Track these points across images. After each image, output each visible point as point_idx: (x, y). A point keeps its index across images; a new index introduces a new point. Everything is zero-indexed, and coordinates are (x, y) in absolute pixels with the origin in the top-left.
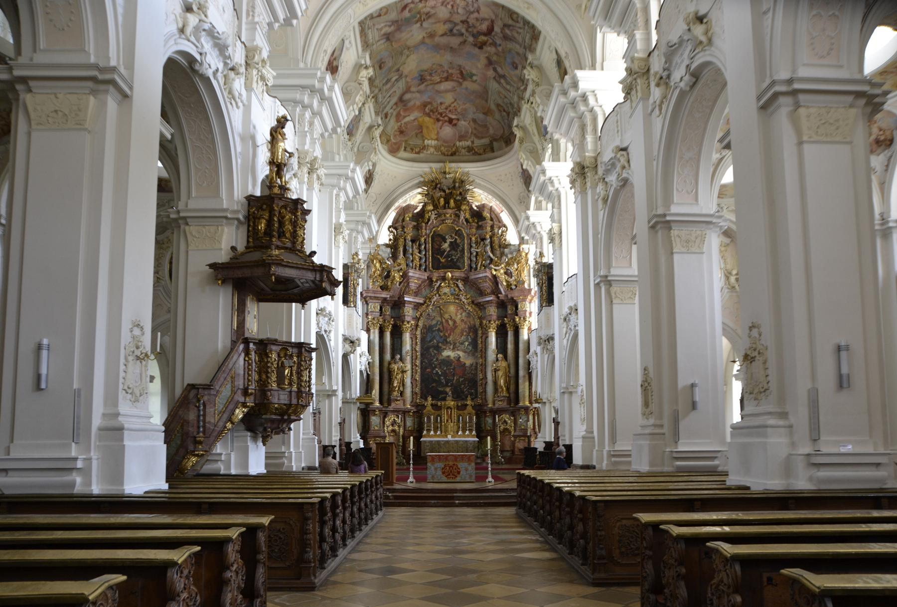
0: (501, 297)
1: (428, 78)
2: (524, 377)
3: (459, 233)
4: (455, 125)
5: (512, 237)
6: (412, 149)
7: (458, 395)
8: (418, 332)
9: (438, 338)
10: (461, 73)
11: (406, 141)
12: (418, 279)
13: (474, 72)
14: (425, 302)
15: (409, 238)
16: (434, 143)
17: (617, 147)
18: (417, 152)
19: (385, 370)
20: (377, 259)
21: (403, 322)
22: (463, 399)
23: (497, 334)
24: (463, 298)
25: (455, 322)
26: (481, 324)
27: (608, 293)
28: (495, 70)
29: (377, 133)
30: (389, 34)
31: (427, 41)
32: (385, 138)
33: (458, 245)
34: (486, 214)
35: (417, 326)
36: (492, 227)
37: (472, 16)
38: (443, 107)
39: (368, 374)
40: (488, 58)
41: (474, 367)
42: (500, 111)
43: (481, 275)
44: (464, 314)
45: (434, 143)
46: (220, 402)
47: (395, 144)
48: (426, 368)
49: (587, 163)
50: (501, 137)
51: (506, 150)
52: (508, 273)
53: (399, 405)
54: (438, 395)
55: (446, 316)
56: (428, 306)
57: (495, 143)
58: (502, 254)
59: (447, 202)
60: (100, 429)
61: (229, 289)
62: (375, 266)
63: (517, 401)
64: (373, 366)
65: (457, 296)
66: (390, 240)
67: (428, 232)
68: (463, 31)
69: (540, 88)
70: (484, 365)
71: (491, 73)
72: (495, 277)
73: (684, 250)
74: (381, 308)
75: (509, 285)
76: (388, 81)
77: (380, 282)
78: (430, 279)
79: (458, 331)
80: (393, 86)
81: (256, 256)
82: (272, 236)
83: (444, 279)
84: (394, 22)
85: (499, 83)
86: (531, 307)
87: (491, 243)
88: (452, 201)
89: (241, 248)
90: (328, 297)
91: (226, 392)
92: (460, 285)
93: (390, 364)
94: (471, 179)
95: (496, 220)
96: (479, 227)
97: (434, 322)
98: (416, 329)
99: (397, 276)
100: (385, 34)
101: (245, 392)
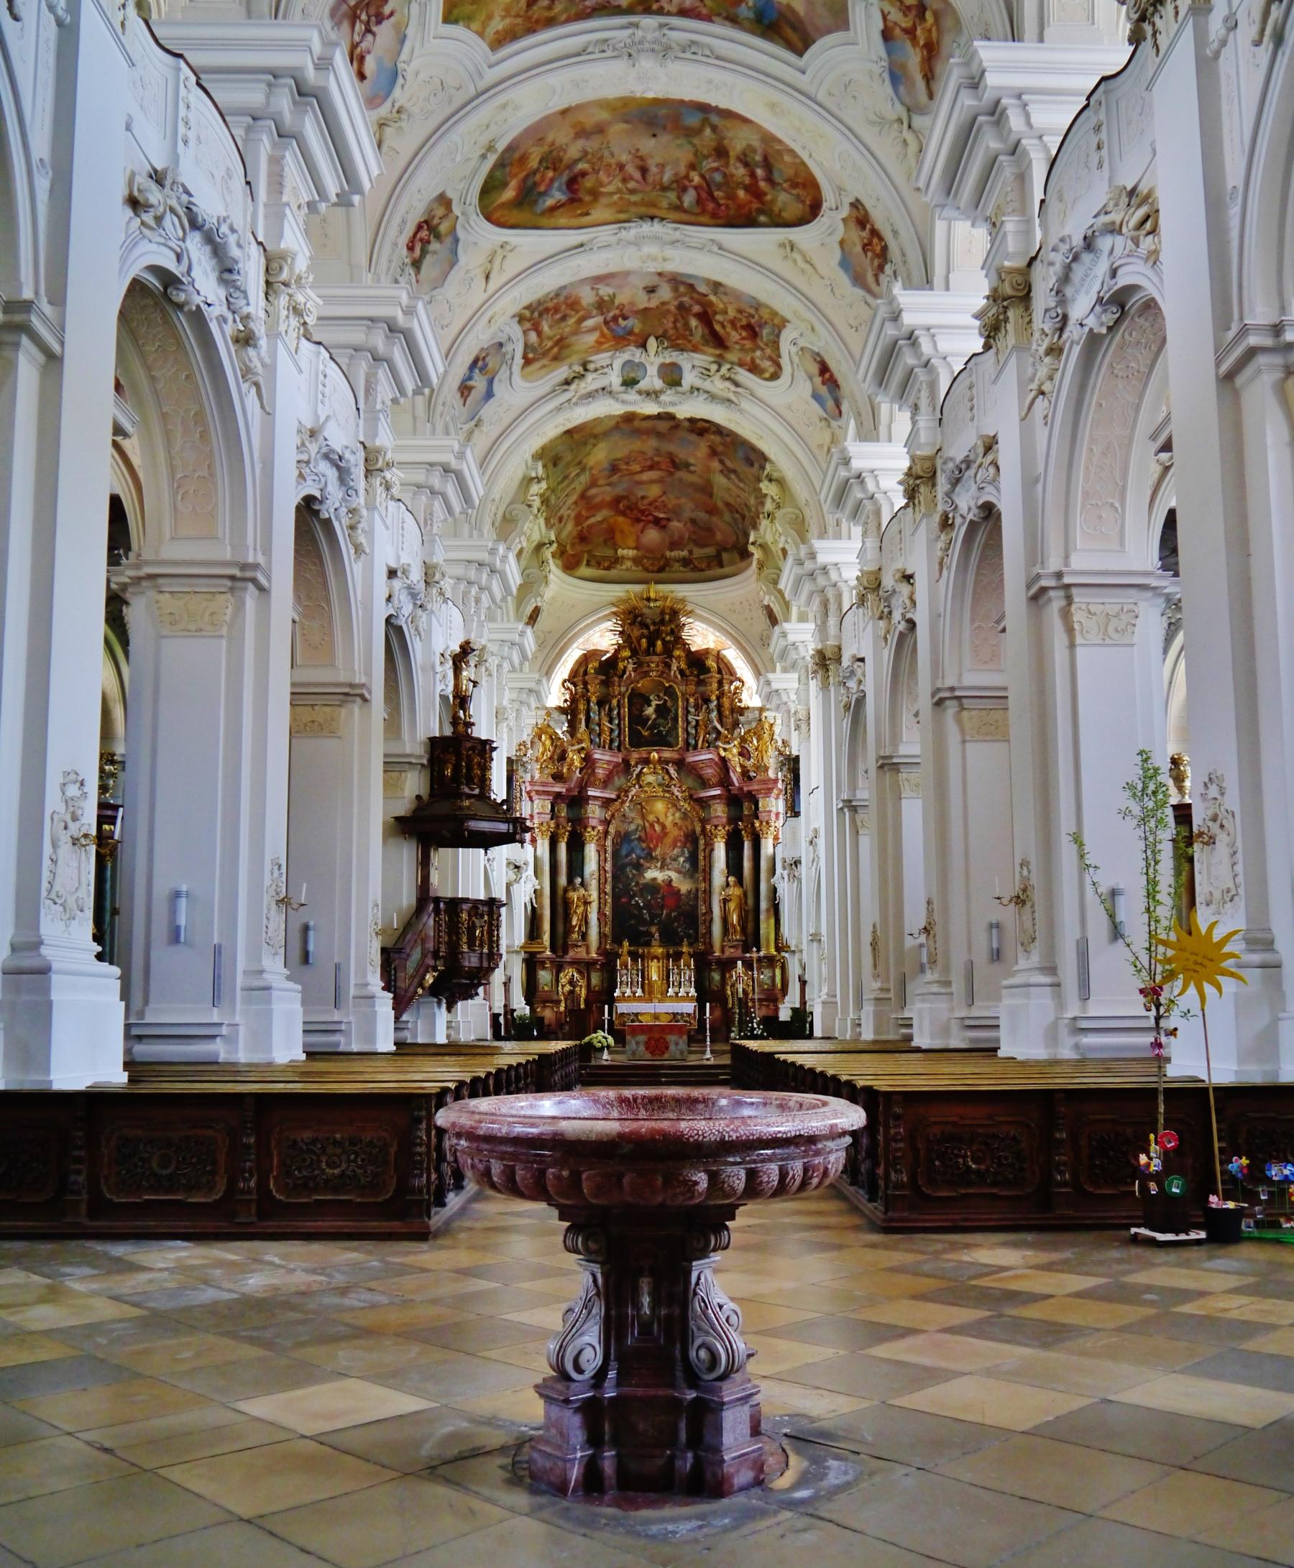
0: (735, 792)
2: (768, 910)
3: (670, 692)
4: (664, 527)
5: (750, 698)
7: (669, 938)
8: (609, 843)
9: (638, 851)
11: (589, 552)
12: (609, 762)
13: (692, 461)
14: (619, 797)
15: (594, 699)
16: (631, 553)
17: (854, 656)
19: (560, 901)
20: (546, 733)
21: (585, 828)
22: (676, 944)
23: (727, 844)
24: (675, 790)
25: (664, 827)
26: (704, 829)
27: (853, 821)
28: (721, 462)
29: (548, 553)
31: (623, 426)
32: (561, 553)
33: (669, 710)
34: (711, 663)
35: (606, 833)
36: (720, 683)
38: (646, 502)
41: (694, 895)
43: (703, 757)
44: (678, 815)
45: (631, 553)
46: (411, 965)
48: (620, 897)
49: (829, 654)
52: (744, 753)
53: (580, 953)
54: (639, 940)
55: (651, 818)
56: (623, 802)
57: (725, 556)
58: (736, 724)
59: (652, 644)
61: (413, 844)
62: (544, 744)
64: (542, 895)
65: (666, 787)
66: (566, 701)
67: (623, 689)
69: (782, 511)
70: (708, 892)
71: (715, 464)
72: (723, 760)
75: (745, 773)
76: (566, 477)
77: (552, 769)
78: (626, 762)
79: (669, 840)
80: (573, 481)
81: (443, 808)
82: (460, 783)
83: (646, 761)
85: (729, 478)
86: (775, 805)
87: (719, 707)
88: (659, 643)
89: (425, 796)
91: (416, 955)
92: (672, 771)
93: (566, 891)
94: (689, 608)
95: (726, 670)
96: (700, 683)
97: (632, 827)
98: (606, 837)
99: (576, 759)
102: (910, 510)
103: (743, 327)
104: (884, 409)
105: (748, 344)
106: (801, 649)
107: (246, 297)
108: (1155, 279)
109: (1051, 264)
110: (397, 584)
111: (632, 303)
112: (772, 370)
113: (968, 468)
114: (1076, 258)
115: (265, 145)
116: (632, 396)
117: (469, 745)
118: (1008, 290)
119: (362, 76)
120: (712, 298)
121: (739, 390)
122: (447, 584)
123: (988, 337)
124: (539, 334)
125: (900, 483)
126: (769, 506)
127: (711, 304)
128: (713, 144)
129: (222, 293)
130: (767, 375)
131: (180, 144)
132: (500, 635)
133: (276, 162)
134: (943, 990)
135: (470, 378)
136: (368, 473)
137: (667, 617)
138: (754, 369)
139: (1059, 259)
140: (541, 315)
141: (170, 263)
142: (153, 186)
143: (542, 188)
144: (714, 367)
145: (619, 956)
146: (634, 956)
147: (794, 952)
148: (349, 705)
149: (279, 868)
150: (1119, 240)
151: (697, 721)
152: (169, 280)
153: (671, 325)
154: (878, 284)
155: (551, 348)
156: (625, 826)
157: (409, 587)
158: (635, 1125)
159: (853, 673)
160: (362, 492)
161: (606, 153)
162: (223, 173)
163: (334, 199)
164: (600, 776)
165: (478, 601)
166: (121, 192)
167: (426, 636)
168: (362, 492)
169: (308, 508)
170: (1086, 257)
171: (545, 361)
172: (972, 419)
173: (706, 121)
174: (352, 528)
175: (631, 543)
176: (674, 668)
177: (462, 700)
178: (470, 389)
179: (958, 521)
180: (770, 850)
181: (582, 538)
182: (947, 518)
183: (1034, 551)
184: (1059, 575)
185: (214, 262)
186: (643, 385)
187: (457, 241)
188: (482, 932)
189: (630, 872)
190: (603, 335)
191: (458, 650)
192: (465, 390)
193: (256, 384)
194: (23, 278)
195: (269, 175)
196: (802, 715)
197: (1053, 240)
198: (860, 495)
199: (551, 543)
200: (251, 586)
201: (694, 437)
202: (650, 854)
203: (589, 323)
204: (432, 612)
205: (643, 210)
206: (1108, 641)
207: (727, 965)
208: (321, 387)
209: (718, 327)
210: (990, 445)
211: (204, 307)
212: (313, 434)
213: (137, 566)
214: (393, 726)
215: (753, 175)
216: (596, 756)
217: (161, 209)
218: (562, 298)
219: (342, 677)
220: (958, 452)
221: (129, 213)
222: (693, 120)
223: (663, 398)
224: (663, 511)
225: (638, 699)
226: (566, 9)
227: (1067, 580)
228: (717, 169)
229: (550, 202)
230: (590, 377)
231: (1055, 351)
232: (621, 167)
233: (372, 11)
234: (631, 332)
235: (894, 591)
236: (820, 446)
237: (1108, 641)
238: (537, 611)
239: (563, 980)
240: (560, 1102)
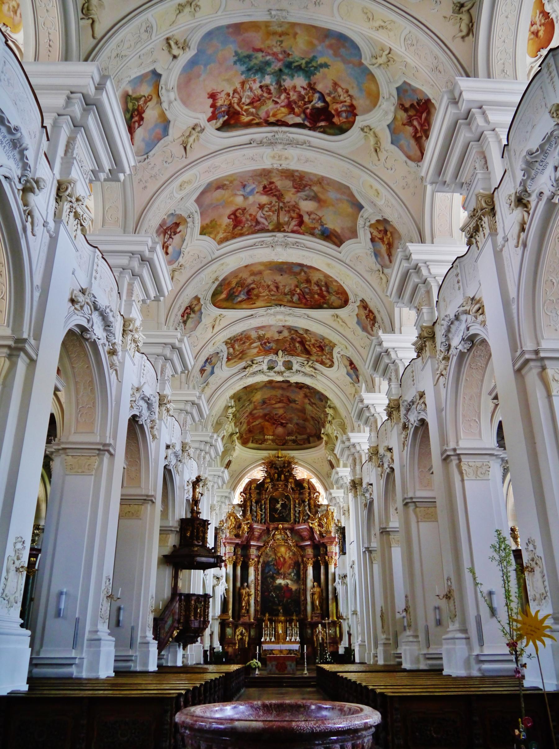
2: (332, 599)
3: (287, 498)
4: (285, 426)
5: (323, 500)
7: (288, 613)
8: (260, 566)
9: (273, 570)
10: (289, 400)
11: (253, 437)
12: (260, 529)
13: (297, 399)
14: (264, 545)
15: (254, 500)
16: (271, 437)
17: (368, 483)
20: (232, 516)
24: (290, 542)
25: (284, 559)
26: (303, 560)
28: (309, 400)
29: (235, 437)
32: (241, 437)
34: (305, 485)
35: (259, 562)
36: (309, 494)
38: (277, 416)
41: (298, 591)
44: (291, 553)
45: (271, 437)
46: (167, 627)
49: (357, 482)
52: (320, 525)
53: (245, 619)
54: (274, 613)
55: (279, 555)
56: (266, 547)
57: (311, 439)
58: (317, 512)
59: (279, 476)
60: (140, 643)
62: (231, 521)
65: (286, 541)
66: (241, 501)
69: (335, 420)
70: (305, 590)
71: (307, 401)
72: (311, 529)
73: (396, 545)
76: (243, 406)
77: (235, 532)
78: (268, 529)
79: (287, 565)
80: (246, 407)
83: (277, 529)
85: (312, 407)
86: (335, 549)
87: (309, 504)
88: (283, 476)
89: (177, 546)
90: (218, 568)
91: (170, 622)
92: (288, 533)
93: (240, 589)
94: (296, 461)
95: (312, 488)
97: (270, 559)
98: (258, 564)
99: (245, 528)
101: (179, 621)
102: (389, 421)
103: (317, 347)
104: (377, 380)
105: (320, 353)
106: (345, 479)
107: (114, 336)
108: (485, 331)
109: (442, 325)
110: (170, 451)
111: (272, 337)
112: (330, 363)
113: (413, 404)
114: (452, 323)
115: (127, 278)
116: (272, 373)
117: (198, 522)
118: (426, 335)
119: (167, 253)
120: (305, 335)
121: (316, 371)
122: (191, 451)
123: (418, 352)
124: (234, 349)
125: (385, 410)
126: (329, 418)
127: (305, 338)
128: (305, 278)
129: (105, 334)
130: (328, 366)
131: (93, 279)
132: (214, 473)
133: (131, 285)
134: (415, 640)
135: (205, 366)
136: (160, 405)
137: (286, 465)
138: (322, 363)
139: (445, 323)
140: (235, 341)
141: (85, 324)
142: (81, 294)
143: (237, 294)
144: (306, 362)
145: (264, 621)
146: (271, 621)
147: (345, 619)
148: (146, 505)
149: (109, 581)
150: (469, 316)
152: (83, 329)
153: (288, 346)
154: (373, 331)
155: (239, 354)
157: (175, 453)
158: (271, 724)
159: (367, 490)
160: (157, 413)
161: (262, 281)
162: (109, 289)
163: (153, 298)
164: (256, 536)
165: (204, 458)
166: (68, 296)
167: (181, 474)
168: (157, 413)
169: (134, 420)
170: (456, 323)
171: (235, 360)
172: (414, 385)
173: (302, 270)
174: (152, 428)
175: (271, 433)
176: (289, 487)
177: (196, 502)
178: (205, 370)
179: (410, 426)
181: (250, 431)
182: (405, 425)
183: (443, 440)
184: (455, 450)
185: (102, 323)
186: (276, 369)
187: (202, 313)
188: (201, 610)
190: (260, 349)
191: (195, 480)
192: (202, 371)
193: (116, 370)
194: (24, 330)
195: (128, 290)
196: (346, 508)
197: (442, 316)
198: (368, 415)
199: (237, 433)
200: (106, 453)
201: (297, 390)
203: (255, 345)
204: (185, 463)
205: (277, 302)
206: (478, 478)
208: (142, 371)
209: (307, 347)
210: (422, 395)
211: (97, 340)
212: (138, 389)
213: (58, 444)
214: (165, 514)
215: (321, 290)
216: (255, 526)
217: (83, 303)
218: (243, 335)
219: (144, 492)
220: (408, 397)
221: (70, 304)
222: (297, 269)
223: (284, 374)
224: (284, 420)
225: (274, 501)
226: (247, 230)
227: (458, 452)
228: (306, 287)
229: (239, 299)
230: (254, 366)
231: (446, 358)
232: (268, 286)
233: (172, 230)
234: (272, 349)
235: (384, 455)
236: (351, 394)
237: (478, 478)
238: (230, 462)
239: (238, 633)
240: (235, 707)
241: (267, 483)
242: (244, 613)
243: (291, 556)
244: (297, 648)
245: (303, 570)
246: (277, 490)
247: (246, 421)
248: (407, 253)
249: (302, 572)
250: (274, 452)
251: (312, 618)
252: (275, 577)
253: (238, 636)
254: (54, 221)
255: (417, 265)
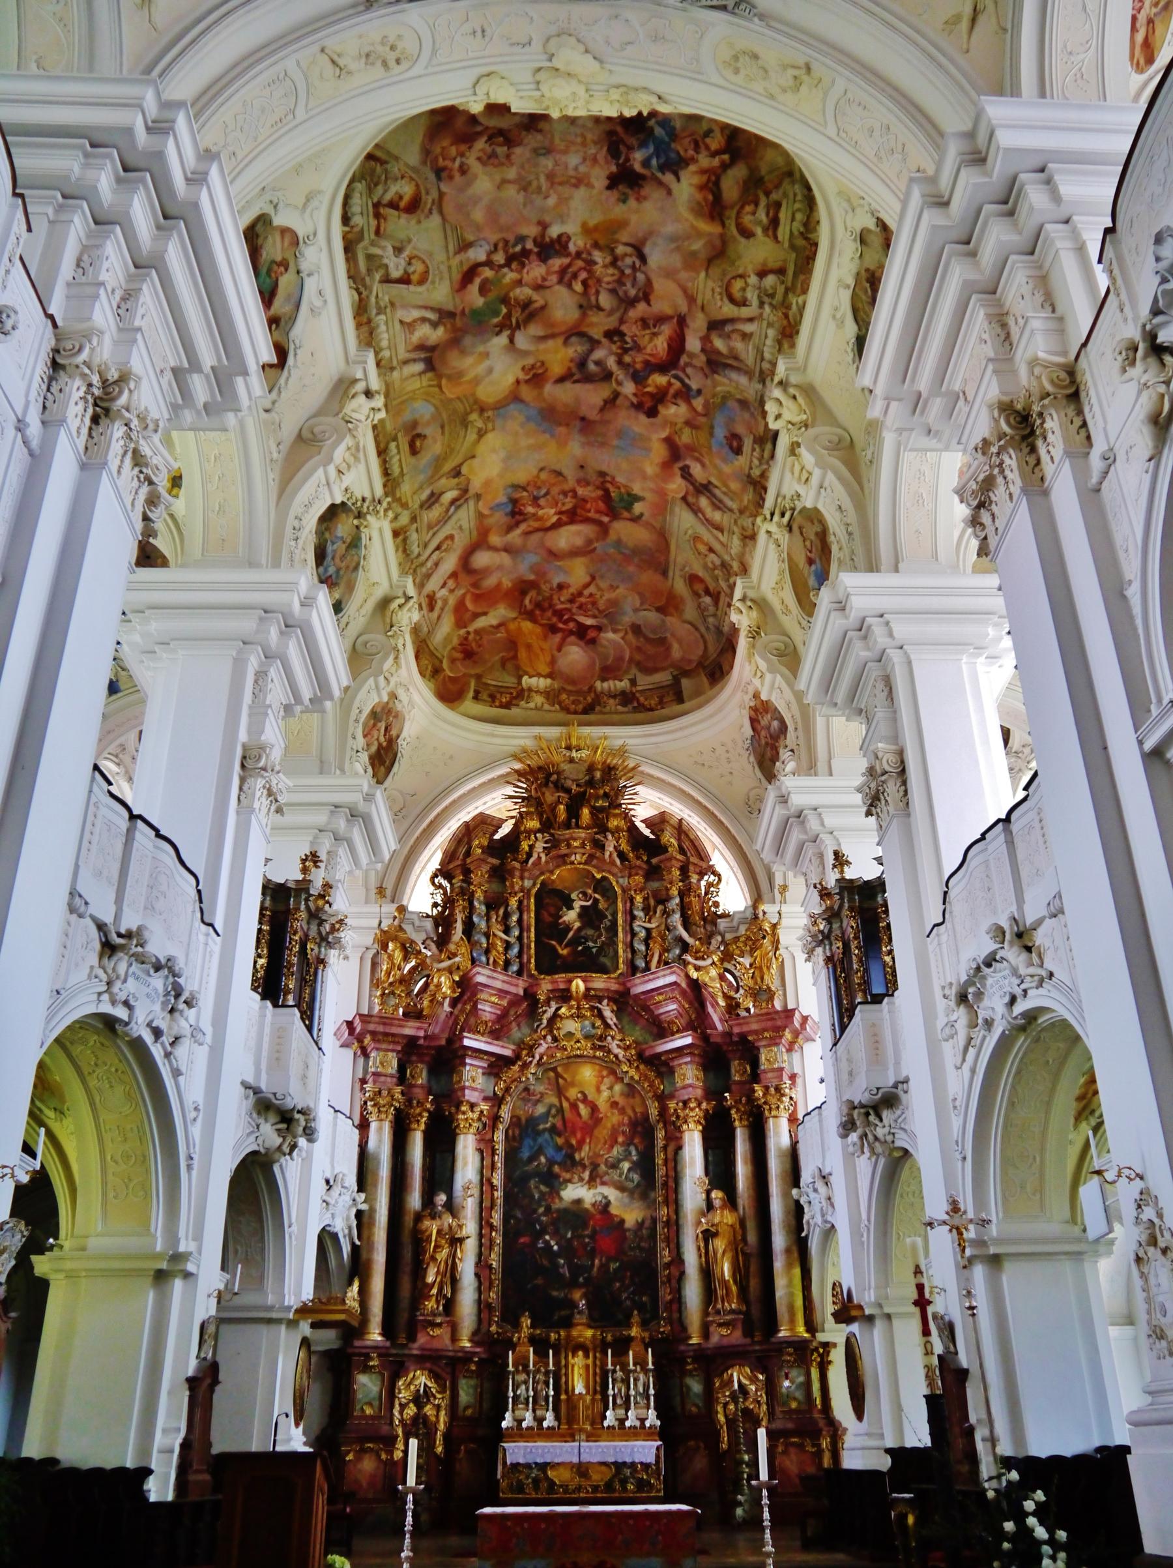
1: (530, 510)
2: (788, 1251)
3: (602, 886)
4: (593, 642)
6: (493, 697)
7: (607, 1313)
8: (499, 1136)
9: (550, 1151)
11: (478, 677)
12: (501, 993)
14: (518, 1057)
15: (479, 894)
16: (543, 683)
18: (504, 701)
19: (406, 1238)
20: (395, 939)
21: (459, 1104)
25: (594, 1109)
30: (433, 349)
33: (601, 916)
36: (684, 871)
37: (633, 314)
39: (355, 1249)
40: (669, 441)
41: (648, 1229)
42: (696, 595)
43: (660, 983)
44: (618, 1088)
45: (543, 683)
47: (453, 680)
48: (518, 1234)
50: (700, 664)
51: (710, 693)
54: (552, 1315)
55: (573, 1093)
56: (526, 1066)
57: (685, 682)
59: (573, 813)
62: (390, 957)
63: (771, 1323)
64: (372, 1223)
66: (435, 905)
68: (611, 363)
70: (675, 1225)
74: (402, 1068)
78: (530, 996)
79: (603, 1132)
83: (564, 996)
84: (445, 316)
87: (684, 908)
88: (586, 811)
92: (608, 1013)
93: (418, 1217)
96: (653, 873)
97: (540, 1110)
98: (494, 1128)
100: (421, 347)
137: (598, 775)
145: (513, 1346)
147: (870, 1319)
151: (648, 931)
156: (529, 1108)
175: (544, 669)
180: (785, 1141)
181: (467, 652)
189: (537, 1189)
202: (571, 1157)
207: (713, 1362)
216: (480, 979)
225: (552, 899)
239: (404, 1395)
241: (529, 832)
242: (434, 1314)
243: (617, 1098)
244: (650, 1458)
245: (665, 1148)
246: (563, 859)
247: (452, 601)
248: (841, 596)
249: (659, 1159)
250: (553, 732)
251: (706, 1334)
252: (557, 1176)
253: (403, 1407)
254: (43, 423)
255: (863, 620)
